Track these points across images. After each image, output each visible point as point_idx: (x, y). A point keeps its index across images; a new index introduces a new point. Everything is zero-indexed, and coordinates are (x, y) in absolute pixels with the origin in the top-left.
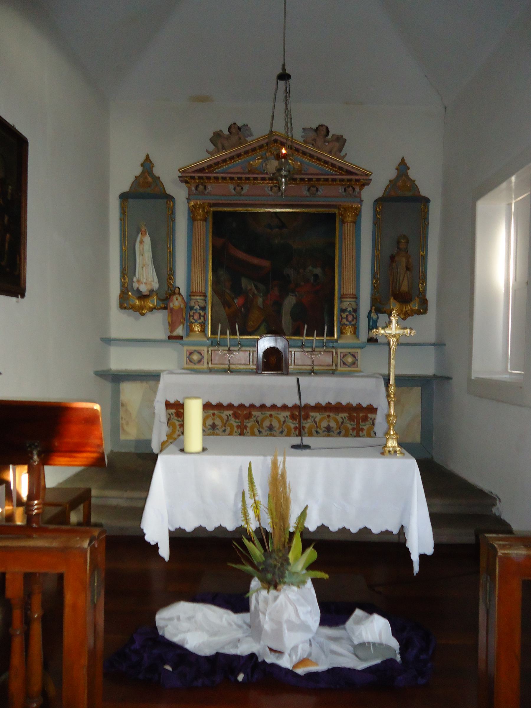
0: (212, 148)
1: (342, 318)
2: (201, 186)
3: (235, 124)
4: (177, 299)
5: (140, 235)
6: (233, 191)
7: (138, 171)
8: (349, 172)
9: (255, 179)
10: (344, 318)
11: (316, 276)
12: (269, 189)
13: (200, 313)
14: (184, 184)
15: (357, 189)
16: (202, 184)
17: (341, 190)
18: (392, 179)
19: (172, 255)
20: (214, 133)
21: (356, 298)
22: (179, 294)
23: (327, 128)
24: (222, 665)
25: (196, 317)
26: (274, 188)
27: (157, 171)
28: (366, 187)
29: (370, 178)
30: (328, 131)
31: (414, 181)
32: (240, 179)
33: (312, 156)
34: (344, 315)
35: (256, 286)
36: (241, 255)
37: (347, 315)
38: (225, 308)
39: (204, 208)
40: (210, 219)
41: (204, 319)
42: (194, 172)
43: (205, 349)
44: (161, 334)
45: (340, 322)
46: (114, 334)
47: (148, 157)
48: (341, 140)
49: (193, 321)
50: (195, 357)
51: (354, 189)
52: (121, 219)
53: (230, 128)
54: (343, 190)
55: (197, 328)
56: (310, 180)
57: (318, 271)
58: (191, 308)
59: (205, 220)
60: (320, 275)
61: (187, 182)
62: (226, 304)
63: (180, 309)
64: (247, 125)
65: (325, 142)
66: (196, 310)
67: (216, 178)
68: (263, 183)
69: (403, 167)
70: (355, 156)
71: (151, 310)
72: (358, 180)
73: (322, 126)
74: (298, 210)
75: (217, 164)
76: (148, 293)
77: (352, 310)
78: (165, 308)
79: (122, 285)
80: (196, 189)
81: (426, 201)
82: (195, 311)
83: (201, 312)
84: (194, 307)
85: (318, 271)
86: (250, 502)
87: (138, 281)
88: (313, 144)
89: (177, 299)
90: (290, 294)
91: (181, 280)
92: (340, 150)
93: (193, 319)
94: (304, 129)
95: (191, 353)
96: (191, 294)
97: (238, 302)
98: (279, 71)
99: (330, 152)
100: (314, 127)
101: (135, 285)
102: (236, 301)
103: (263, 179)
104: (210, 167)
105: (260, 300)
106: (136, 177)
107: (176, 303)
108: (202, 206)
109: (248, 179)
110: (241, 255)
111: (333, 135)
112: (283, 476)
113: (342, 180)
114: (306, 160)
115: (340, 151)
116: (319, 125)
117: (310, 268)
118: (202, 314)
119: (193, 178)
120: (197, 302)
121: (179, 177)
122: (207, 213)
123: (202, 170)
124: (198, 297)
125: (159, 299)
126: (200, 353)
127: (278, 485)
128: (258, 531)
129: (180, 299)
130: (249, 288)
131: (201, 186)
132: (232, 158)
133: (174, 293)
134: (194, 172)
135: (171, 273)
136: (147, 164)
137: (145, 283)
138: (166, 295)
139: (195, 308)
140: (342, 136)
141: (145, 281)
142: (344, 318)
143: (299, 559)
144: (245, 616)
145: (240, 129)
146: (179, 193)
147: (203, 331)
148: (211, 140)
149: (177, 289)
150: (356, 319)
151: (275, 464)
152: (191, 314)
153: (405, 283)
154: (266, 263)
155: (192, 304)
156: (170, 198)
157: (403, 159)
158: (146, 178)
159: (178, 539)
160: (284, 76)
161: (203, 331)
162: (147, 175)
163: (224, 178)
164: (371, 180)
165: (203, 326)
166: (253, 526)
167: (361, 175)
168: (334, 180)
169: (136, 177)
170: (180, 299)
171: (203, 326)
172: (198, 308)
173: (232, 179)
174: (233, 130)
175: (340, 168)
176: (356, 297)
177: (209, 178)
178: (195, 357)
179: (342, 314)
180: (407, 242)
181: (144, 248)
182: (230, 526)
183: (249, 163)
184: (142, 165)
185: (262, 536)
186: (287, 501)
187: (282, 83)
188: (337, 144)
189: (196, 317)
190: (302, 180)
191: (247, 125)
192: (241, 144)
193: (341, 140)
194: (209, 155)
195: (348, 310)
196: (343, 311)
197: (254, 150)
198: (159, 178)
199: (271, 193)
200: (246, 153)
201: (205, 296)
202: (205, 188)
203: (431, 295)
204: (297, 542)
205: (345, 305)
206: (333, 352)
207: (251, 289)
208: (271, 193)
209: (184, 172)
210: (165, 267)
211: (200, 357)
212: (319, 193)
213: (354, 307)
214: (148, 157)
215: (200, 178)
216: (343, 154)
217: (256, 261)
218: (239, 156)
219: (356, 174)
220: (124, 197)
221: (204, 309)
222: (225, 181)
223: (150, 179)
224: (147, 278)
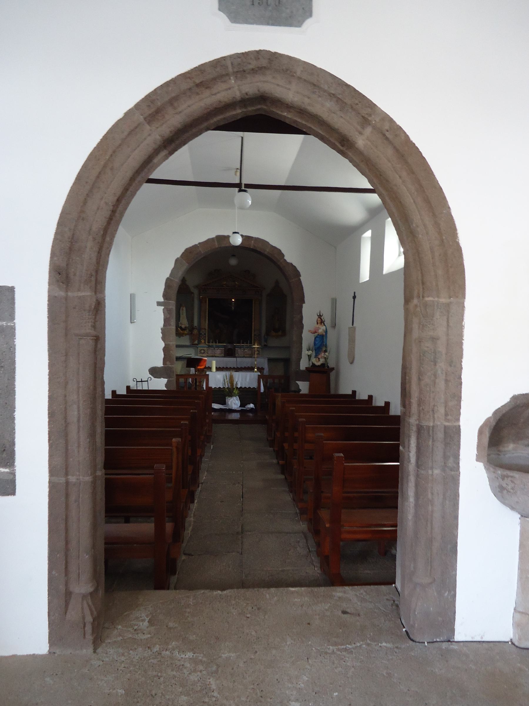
19: (193, 314)
44: (188, 343)
55: (203, 341)
58: (201, 334)
71: (186, 335)
86: (226, 381)
87: (181, 324)
91: (196, 324)
101: (180, 325)
107: (195, 332)
125: (189, 330)
127: (231, 378)
128: (228, 388)
135: (192, 321)
138: (191, 329)
146: (196, 292)
147: (205, 342)
155: (201, 332)
156: (193, 293)
161: (205, 342)
165: (205, 340)
166: (227, 386)
171: (205, 340)
178: (202, 351)
196: (255, 335)
204: (235, 389)
210: (190, 319)
221: (205, 334)
224: (184, 323)
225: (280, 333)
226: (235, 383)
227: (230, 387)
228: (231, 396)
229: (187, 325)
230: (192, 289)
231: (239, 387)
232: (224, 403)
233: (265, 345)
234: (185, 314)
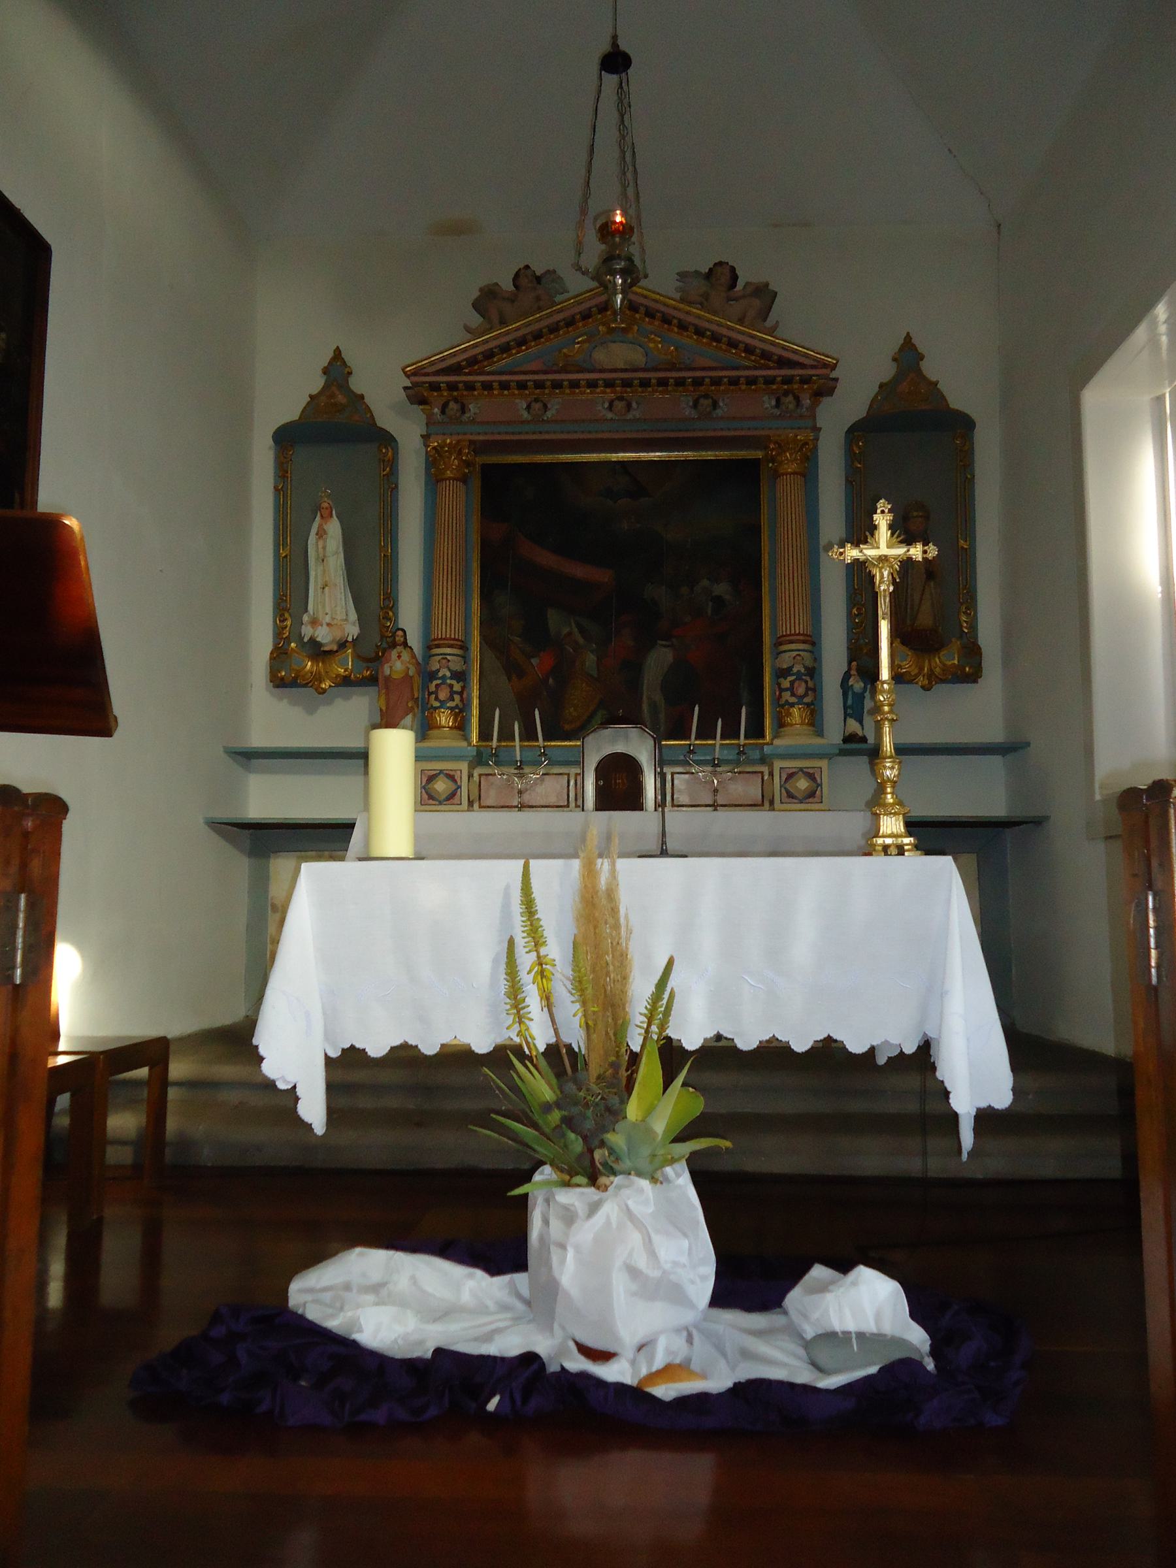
0: (476, 320)
1: (782, 690)
2: (452, 405)
3: (527, 267)
4: (399, 657)
5: (318, 518)
6: (525, 415)
7: (316, 383)
8: (782, 362)
9: (574, 385)
10: (787, 690)
11: (719, 601)
12: (606, 405)
13: (451, 686)
14: (417, 408)
15: (807, 402)
16: (456, 400)
17: (769, 402)
18: (885, 381)
20: (481, 290)
21: (813, 644)
22: (405, 644)
23: (733, 269)
24: (449, 1381)
25: (443, 695)
26: (617, 403)
27: (358, 384)
28: (826, 400)
29: (833, 375)
30: (734, 278)
31: (936, 384)
32: (539, 385)
33: (700, 332)
34: (786, 683)
35: (582, 631)
36: (546, 559)
37: (792, 683)
38: (509, 679)
39: (460, 453)
40: (476, 483)
41: (462, 700)
42: (438, 373)
43: (464, 766)
45: (777, 701)
46: (258, 740)
47: (338, 353)
48: (764, 295)
49: (437, 704)
50: (441, 786)
51: (797, 399)
52: (276, 488)
53: (517, 276)
54: (773, 403)
55: (444, 719)
56: (698, 382)
57: (722, 589)
58: (433, 676)
59: (464, 480)
60: (727, 597)
61: (422, 401)
62: (513, 669)
63: (407, 678)
64: (554, 272)
65: (729, 299)
66: (444, 677)
67: (487, 386)
68: (591, 393)
69: (909, 355)
70: (799, 327)
72: (805, 380)
73: (720, 264)
74: (675, 455)
75: (489, 355)
76: (335, 648)
77: (803, 670)
78: (372, 681)
79: (278, 633)
80: (443, 412)
81: (964, 424)
82: (439, 682)
83: (454, 682)
84: (438, 671)
85: (722, 589)
86: (526, 960)
87: (314, 622)
88: (701, 304)
89: (399, 657)
90: (660, 642)
92: (765, 313)
93: (437, 699)
94: (683, 275)
95: (431, 779)
96: (430, 645)
97: (538, 664)
98: (605, 47)
99: (741, 321)
100: (705, 270)
102: (535, 661)
103: (592, 384)
104: (472, 361)
105: (591, 659)
106: (311, 396)
107: (397, 665)
108: (456, 449)
109: (557, 385)
110: (546, 559)
111: (747, 284)
112: (611, 894)
113: (769, 381)
114: (688, 340)
115: (765, 320)
116: (715, 264)
117: (705, 582)
118: (457, 687)
119: (435, 387)
120: (446, 661)
121: (405, 388)
122: (468, 464)
123: (456, 369)
124: (448, 650)
126: (451, 778)
127: (597, 915)
128: (552, 1052)
129: (406, 656)
130: (565, 630)
131: (452, 405)
132: (522, 342)
133: (394, 645)
134: (438, 373)
136: (337, 370)
137: (328, 625)
139: (440, 674)
140: (767, 285)
141: (327, 619)
142: (787, 690)
143: (656, 1108)
144: (520, 1279)
145: (538, 279)
147: (461, 726)
148: (476, 306)
149: (400, 633)
150: (815, 690)
151: (597, 915)
152: (432, 688)
153: (926, 606)
154: (602, 576)
156: (386, 439)
157: (908, 338)
158: (332, 396)
159: (347, 1068)
160: (616, 61)
161: (461, 726)
162: (334, 389)
163: (504, 386)
164: (836, 380)
166: (541, 1037)
167: (813, 367)
168: (751, 381)
169: (311, 396)
170: (406, 656)
172: (448, 674)
173: (522, 386)
174: (523, 281)
175: (765, 355)
176: (813, 641)
177: (470, 387)
179: (781, 680)
180: (927, 518)
181: (327, 547)
182: (482, 1045)
183: (560, 352)
184: (326, 371)
185: (559, 1057)
186: (622, 959)
187: (611, 80)
188: (757, 303)
189: (443, 695)
190: (680, 383)
191: (554, 272)
192: (540, 309)
193: (764, 295)
194: (469, 336)
195: (795, 670)
197: (570, 322)
198: (362, 397)
199: (610, 415)
200: (554, 329)
201: (464, 647)
202: (463, 410)
203: (989, 633)
204: (650, 1070)
205: (785, 661)
206: (762, 773)
207: (570, 634)
208: (610, 415)
209: (415, 373)
210: (373, 587)
211: (452, 786)
212: (719, 412)
213: (809, 663)
214: (338, 353)
215: (452, 387)
216: (769, 323)
217: (579, 571)
218: (538, 336)
219: (802, 366)
220: (286, 438)
221: (460, 676)
222: (506, 392)
223: (341, 398)
224: (332, 612)
225: (951, 658)
226: (640, 990)
227: (575, 1036)
228: (591, 1171)
229: (353, 631)
230: (387, 420)
231: (692, 1042)
232: (498, 1244)
233: (849, 739)
234: (336, 563)
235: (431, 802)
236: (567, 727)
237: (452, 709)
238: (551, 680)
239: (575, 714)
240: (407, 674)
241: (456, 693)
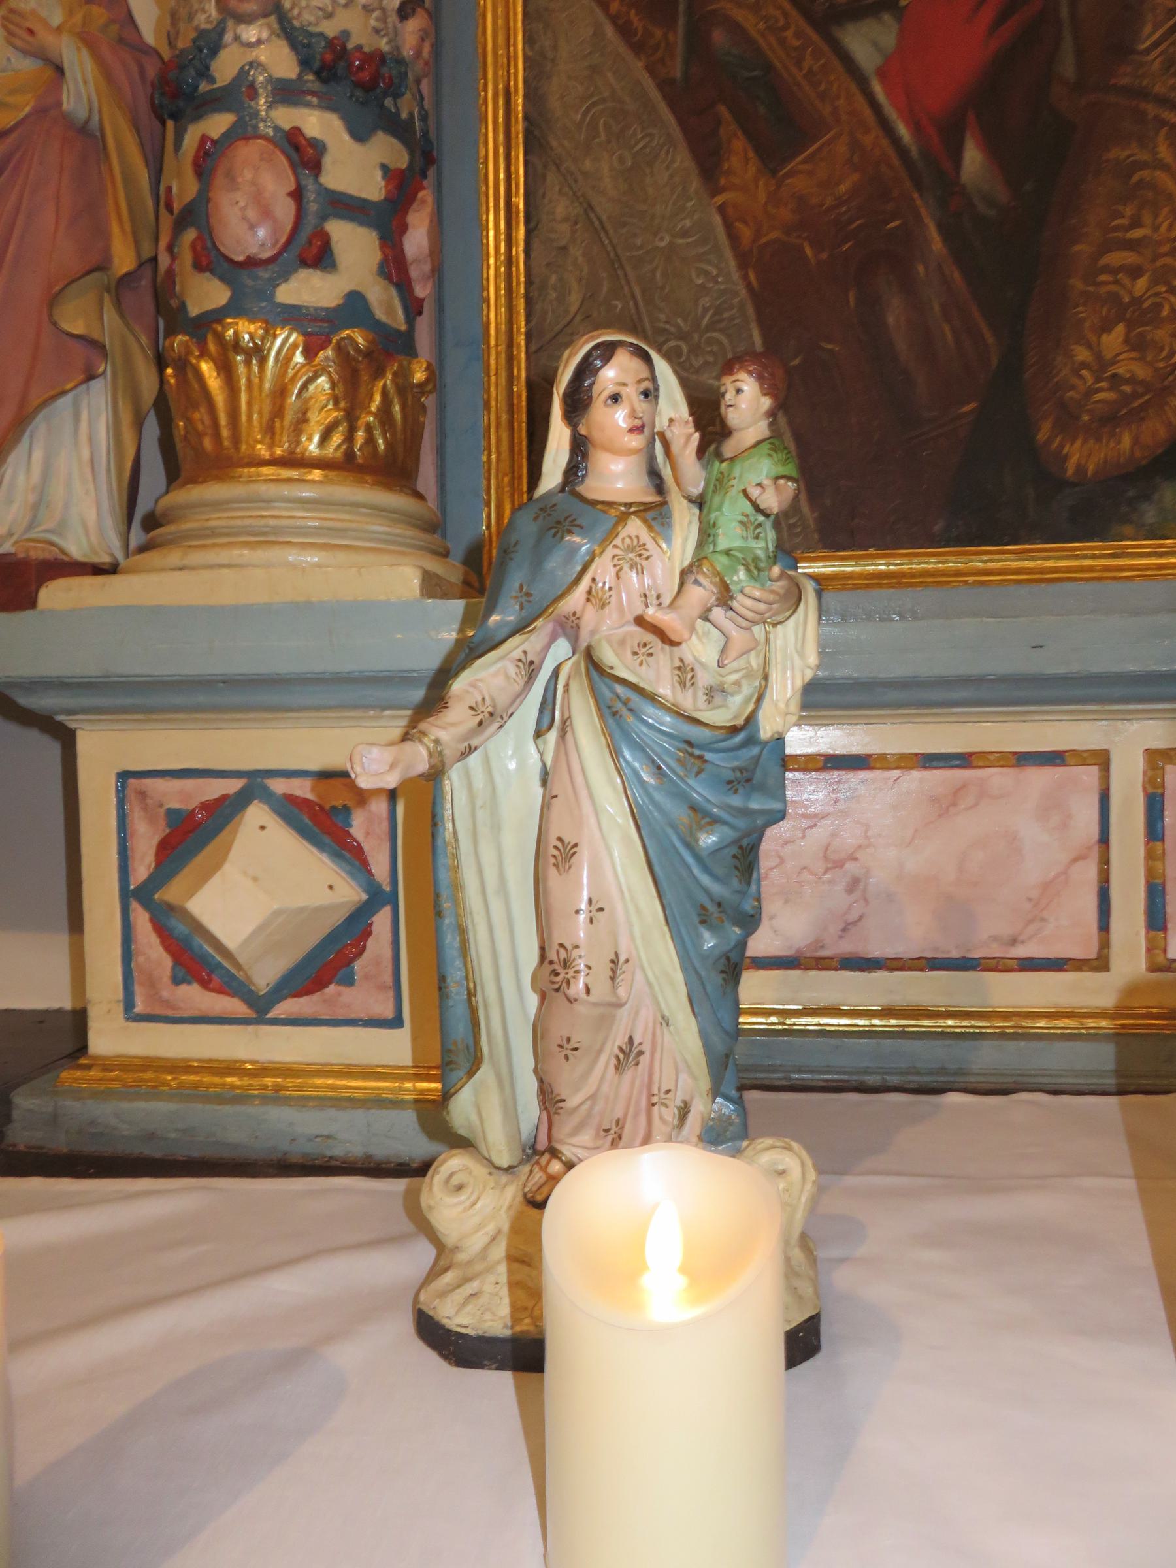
25: (252, 212)
38: (710, 164)
41: (394, 268)
83: (315, 122)
95: (192, 835)
102: (868, 42)
118: (356, 166)
139: (225, 67)
172: (280, 61)
235: (194, 996)
236: (1082, 456)
237: (317, 328)
238: (973, 158)
239: (1129, 367)
240: (47, 110)
241: (346, 206)
